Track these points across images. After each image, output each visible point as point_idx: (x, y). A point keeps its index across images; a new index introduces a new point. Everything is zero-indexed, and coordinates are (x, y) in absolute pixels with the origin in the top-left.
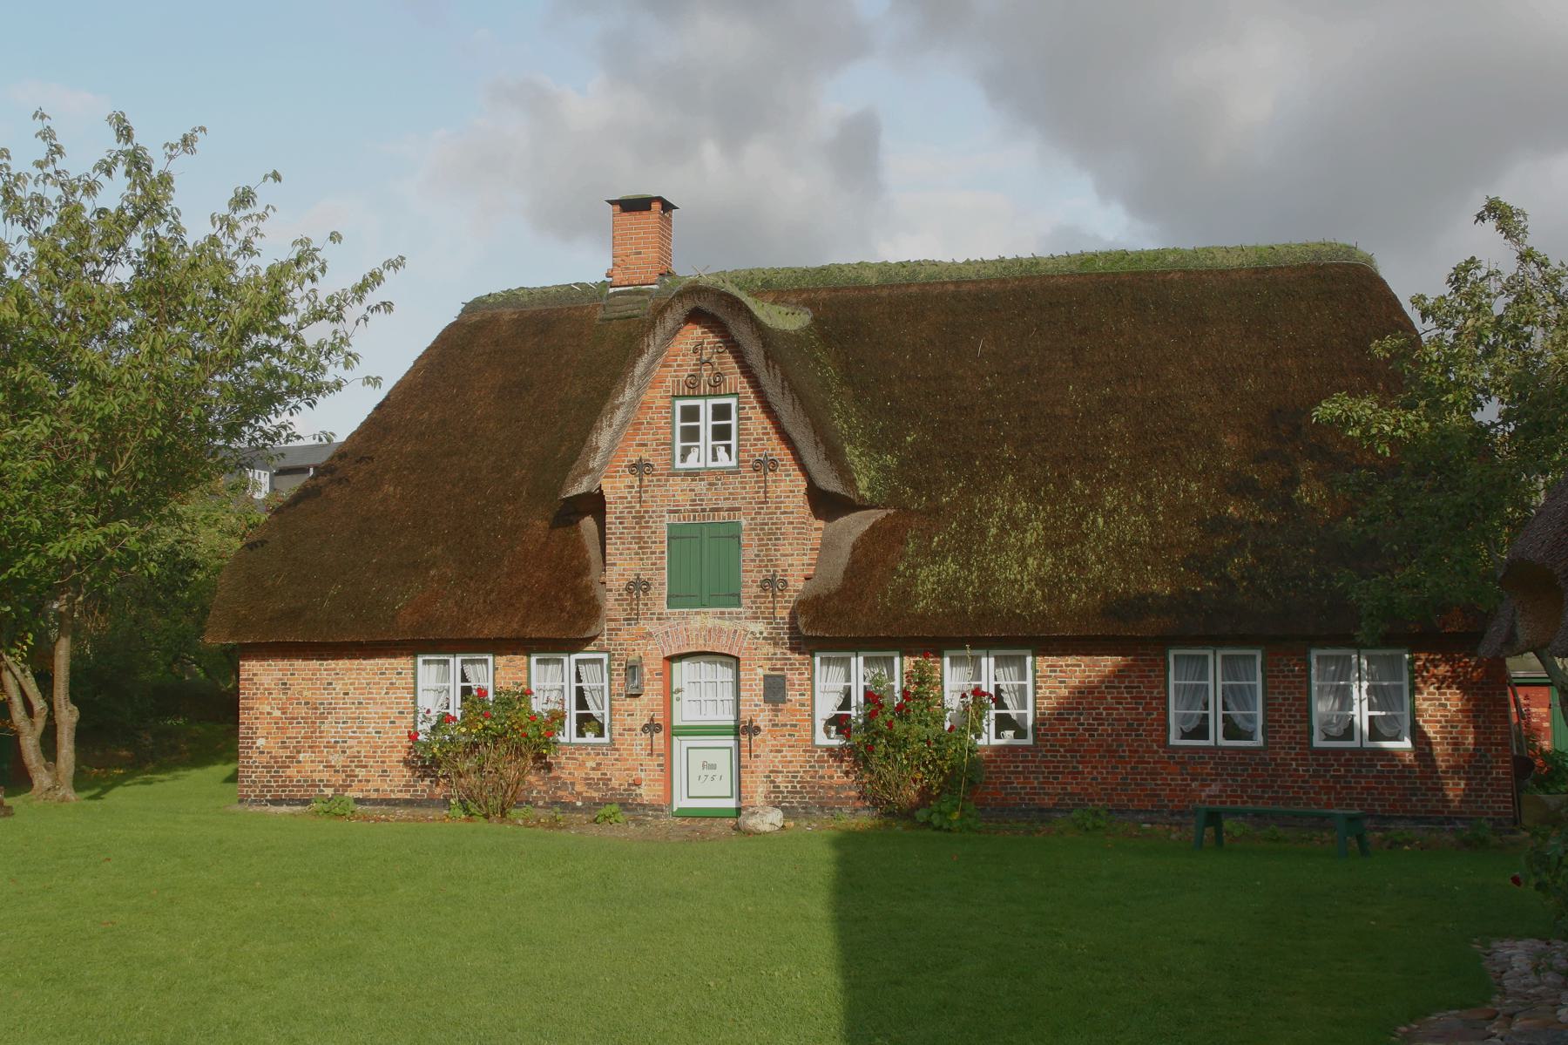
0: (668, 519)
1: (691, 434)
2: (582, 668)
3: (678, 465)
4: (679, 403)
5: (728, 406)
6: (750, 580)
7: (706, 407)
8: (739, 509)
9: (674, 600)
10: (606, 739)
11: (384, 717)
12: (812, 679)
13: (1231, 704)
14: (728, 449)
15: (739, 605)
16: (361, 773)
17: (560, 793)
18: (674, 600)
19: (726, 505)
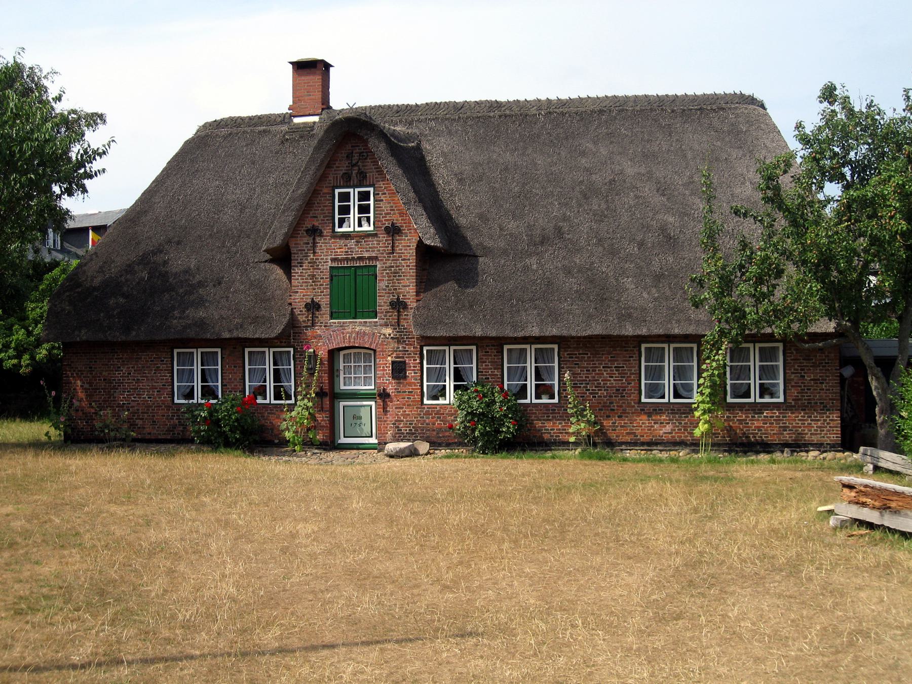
0: (330, 264)
1: (345, 210)
2: (278, 357)
6: (383, 302)
8: (376, 258)
12: (421, 363)
16: (140, 422)
19: (366, 255)
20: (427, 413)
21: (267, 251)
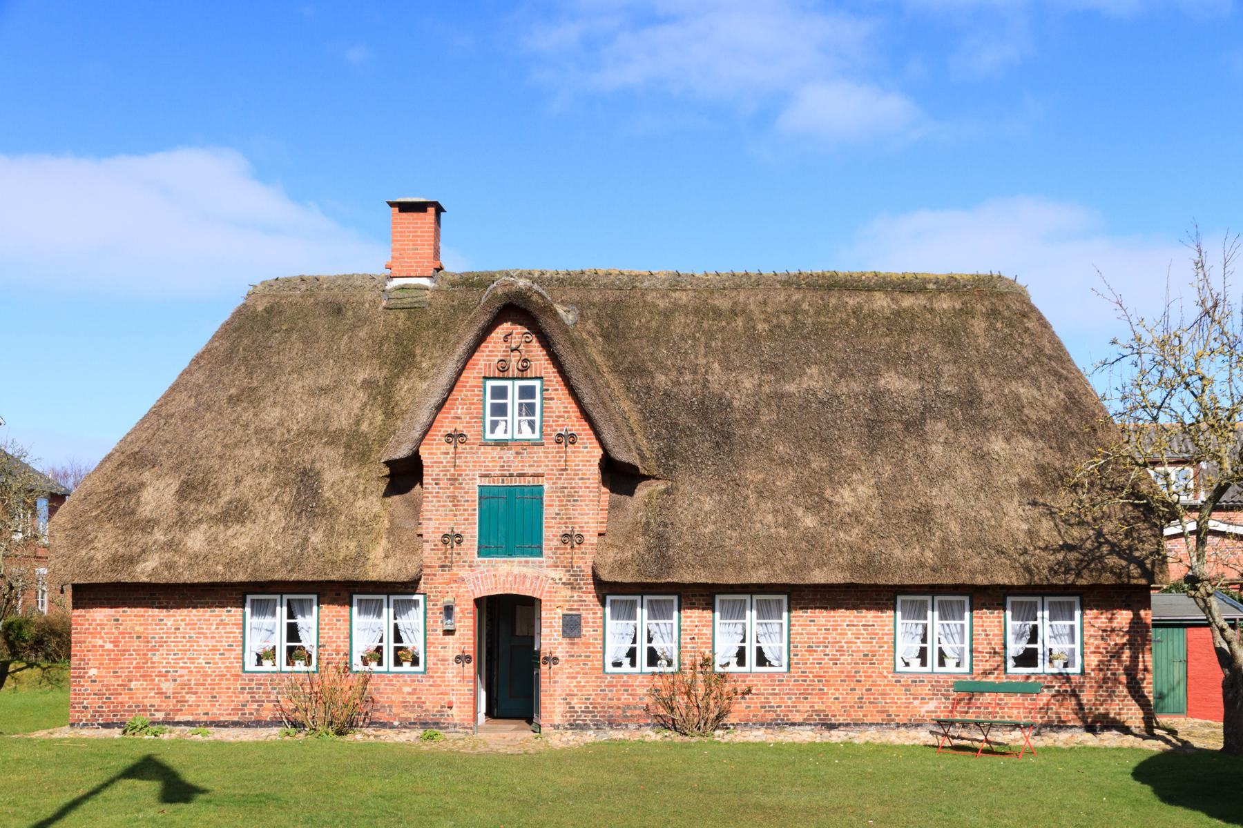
0: (478, 482)
1: (500, 410)
3: (489, 436)
4: (490, 384)
5: (533, 388)
6: (551, 534)
7: (513, 387)
8: (542, 475)
9: (484, 550)
10: (421, 668)
11: (214, 649)
12: (604, 617)
13: (943, 640)
14: (532, 424)
15: (540, 554)
16: (191, 699)
17: (378, 714)
18: (484, 550)
19: (531, 471)
20: (611, 685)
21: (388, 463)
